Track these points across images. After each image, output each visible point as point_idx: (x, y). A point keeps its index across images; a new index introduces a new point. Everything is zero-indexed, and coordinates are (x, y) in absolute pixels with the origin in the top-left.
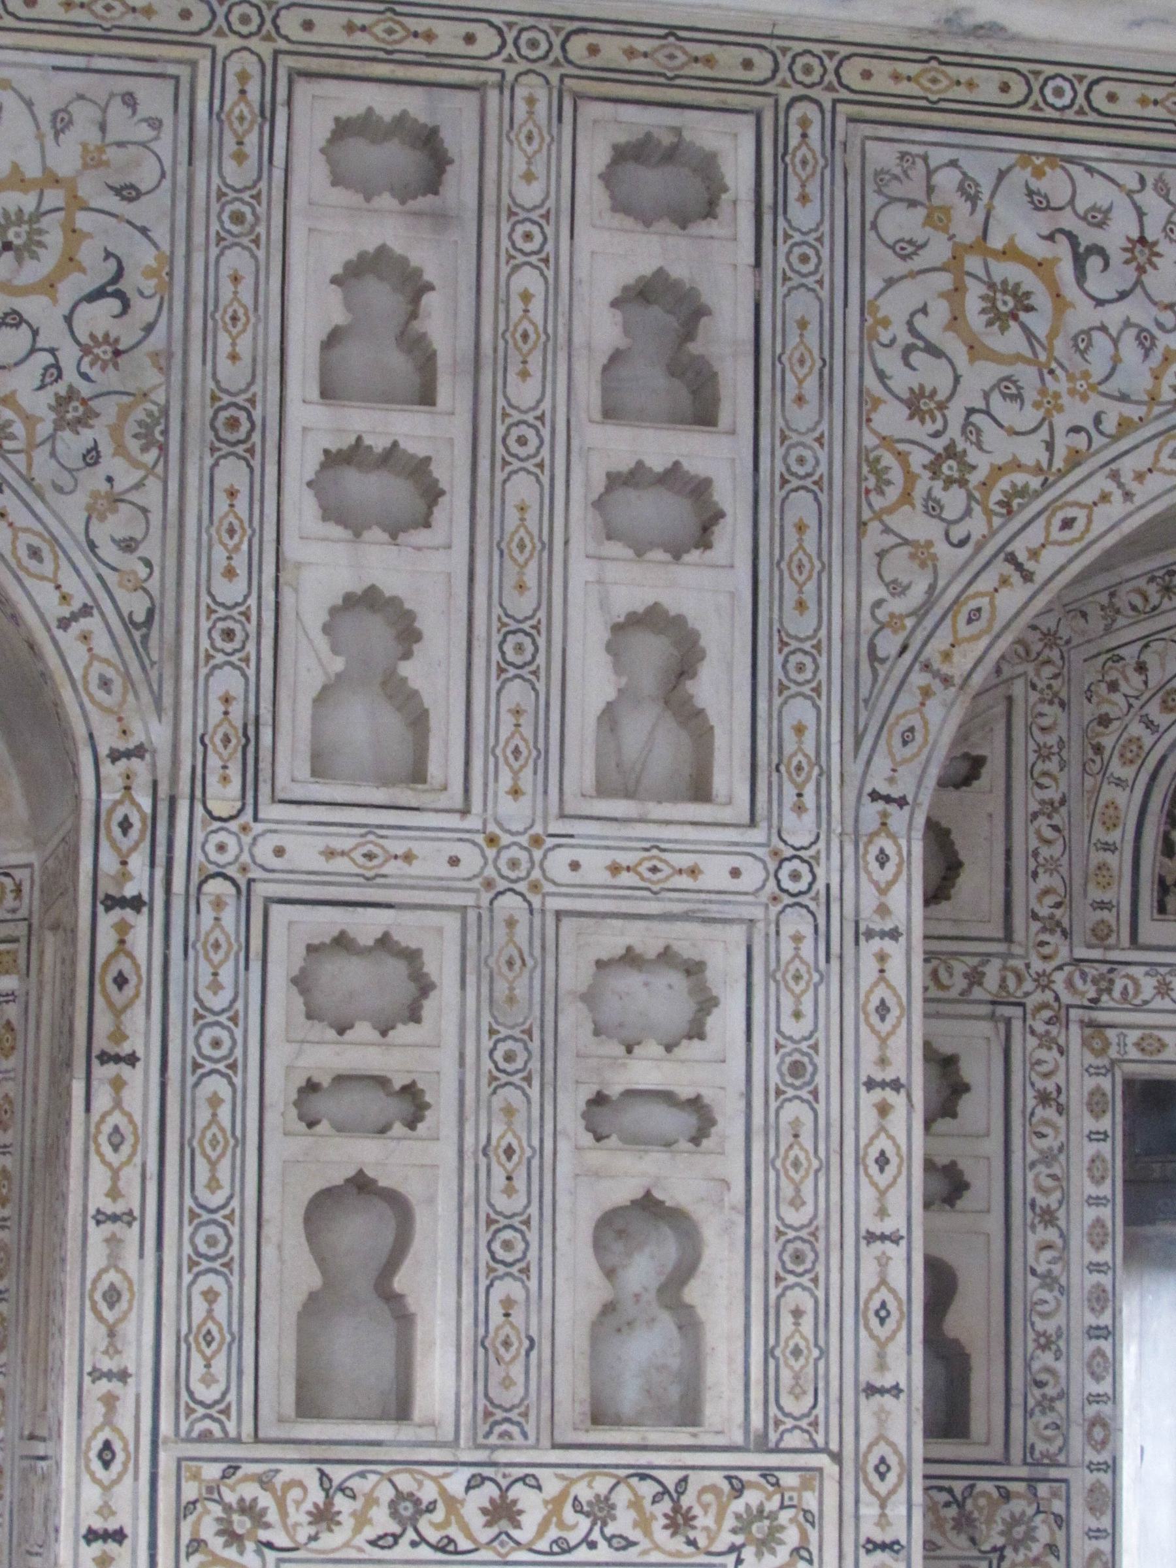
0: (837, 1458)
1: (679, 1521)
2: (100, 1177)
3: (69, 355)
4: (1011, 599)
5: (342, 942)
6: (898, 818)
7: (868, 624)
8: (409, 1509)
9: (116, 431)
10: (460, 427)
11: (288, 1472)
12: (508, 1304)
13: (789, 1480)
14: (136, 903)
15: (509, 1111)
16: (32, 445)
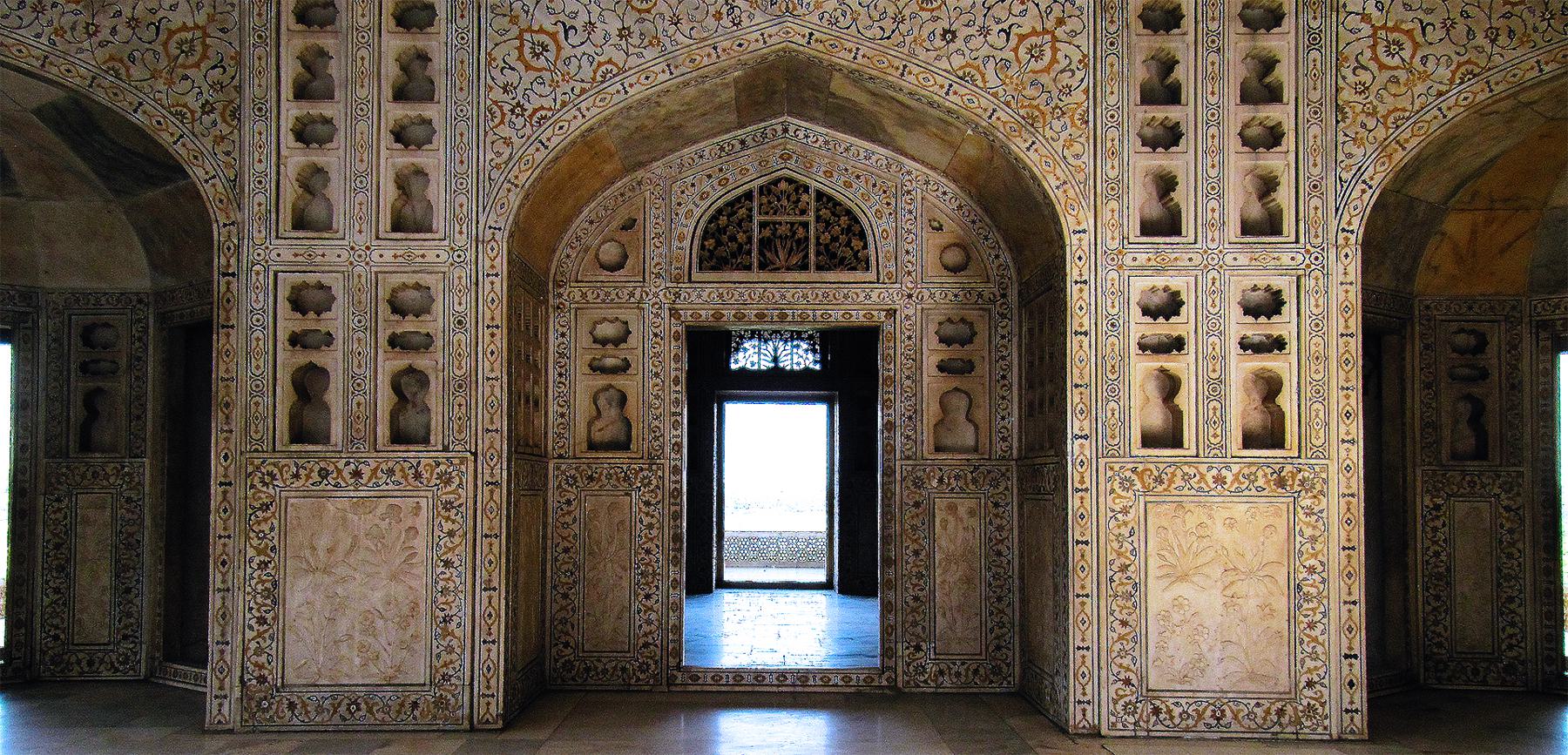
0: (475, 454)
1: (418, 476)
2: (222, 367)
3: (205, 88)
4: (539, 157)
5: (305, 285)
6: (498, 235)
7: (488, 167)
8: (324, 474)
9: (222, 115)
10: (341, 105)
11: (283, 462)
12: (359, 404)
13: (456, 461)
14: (233, 275)
15: (359, 340)
16: (194, 120)
